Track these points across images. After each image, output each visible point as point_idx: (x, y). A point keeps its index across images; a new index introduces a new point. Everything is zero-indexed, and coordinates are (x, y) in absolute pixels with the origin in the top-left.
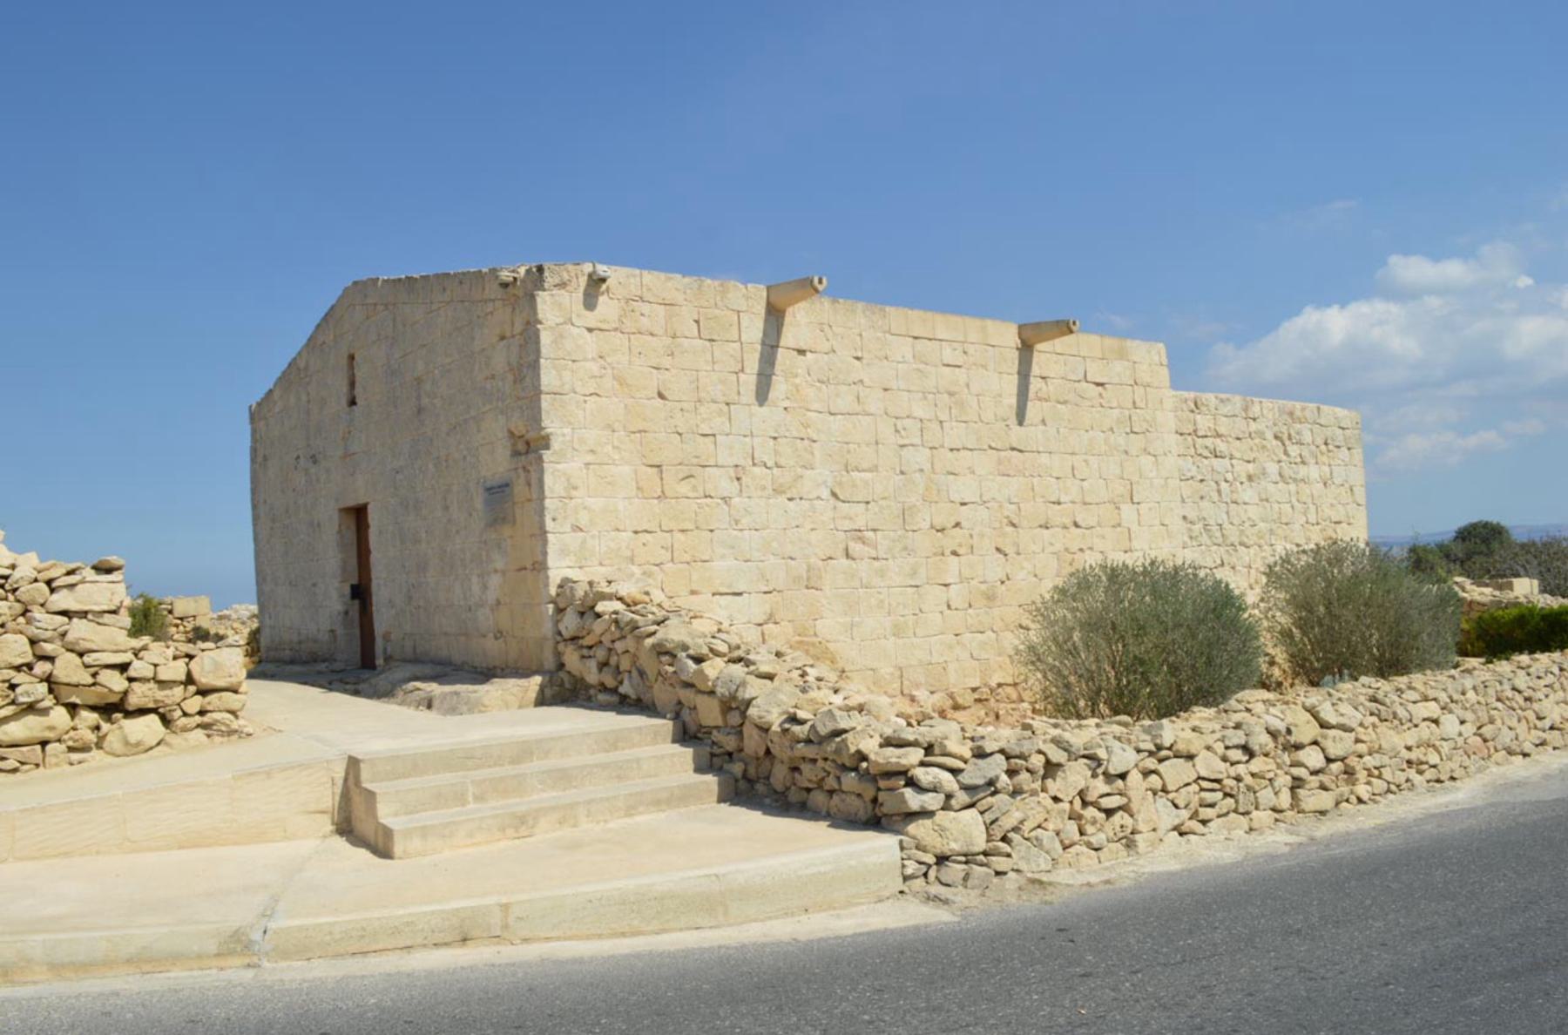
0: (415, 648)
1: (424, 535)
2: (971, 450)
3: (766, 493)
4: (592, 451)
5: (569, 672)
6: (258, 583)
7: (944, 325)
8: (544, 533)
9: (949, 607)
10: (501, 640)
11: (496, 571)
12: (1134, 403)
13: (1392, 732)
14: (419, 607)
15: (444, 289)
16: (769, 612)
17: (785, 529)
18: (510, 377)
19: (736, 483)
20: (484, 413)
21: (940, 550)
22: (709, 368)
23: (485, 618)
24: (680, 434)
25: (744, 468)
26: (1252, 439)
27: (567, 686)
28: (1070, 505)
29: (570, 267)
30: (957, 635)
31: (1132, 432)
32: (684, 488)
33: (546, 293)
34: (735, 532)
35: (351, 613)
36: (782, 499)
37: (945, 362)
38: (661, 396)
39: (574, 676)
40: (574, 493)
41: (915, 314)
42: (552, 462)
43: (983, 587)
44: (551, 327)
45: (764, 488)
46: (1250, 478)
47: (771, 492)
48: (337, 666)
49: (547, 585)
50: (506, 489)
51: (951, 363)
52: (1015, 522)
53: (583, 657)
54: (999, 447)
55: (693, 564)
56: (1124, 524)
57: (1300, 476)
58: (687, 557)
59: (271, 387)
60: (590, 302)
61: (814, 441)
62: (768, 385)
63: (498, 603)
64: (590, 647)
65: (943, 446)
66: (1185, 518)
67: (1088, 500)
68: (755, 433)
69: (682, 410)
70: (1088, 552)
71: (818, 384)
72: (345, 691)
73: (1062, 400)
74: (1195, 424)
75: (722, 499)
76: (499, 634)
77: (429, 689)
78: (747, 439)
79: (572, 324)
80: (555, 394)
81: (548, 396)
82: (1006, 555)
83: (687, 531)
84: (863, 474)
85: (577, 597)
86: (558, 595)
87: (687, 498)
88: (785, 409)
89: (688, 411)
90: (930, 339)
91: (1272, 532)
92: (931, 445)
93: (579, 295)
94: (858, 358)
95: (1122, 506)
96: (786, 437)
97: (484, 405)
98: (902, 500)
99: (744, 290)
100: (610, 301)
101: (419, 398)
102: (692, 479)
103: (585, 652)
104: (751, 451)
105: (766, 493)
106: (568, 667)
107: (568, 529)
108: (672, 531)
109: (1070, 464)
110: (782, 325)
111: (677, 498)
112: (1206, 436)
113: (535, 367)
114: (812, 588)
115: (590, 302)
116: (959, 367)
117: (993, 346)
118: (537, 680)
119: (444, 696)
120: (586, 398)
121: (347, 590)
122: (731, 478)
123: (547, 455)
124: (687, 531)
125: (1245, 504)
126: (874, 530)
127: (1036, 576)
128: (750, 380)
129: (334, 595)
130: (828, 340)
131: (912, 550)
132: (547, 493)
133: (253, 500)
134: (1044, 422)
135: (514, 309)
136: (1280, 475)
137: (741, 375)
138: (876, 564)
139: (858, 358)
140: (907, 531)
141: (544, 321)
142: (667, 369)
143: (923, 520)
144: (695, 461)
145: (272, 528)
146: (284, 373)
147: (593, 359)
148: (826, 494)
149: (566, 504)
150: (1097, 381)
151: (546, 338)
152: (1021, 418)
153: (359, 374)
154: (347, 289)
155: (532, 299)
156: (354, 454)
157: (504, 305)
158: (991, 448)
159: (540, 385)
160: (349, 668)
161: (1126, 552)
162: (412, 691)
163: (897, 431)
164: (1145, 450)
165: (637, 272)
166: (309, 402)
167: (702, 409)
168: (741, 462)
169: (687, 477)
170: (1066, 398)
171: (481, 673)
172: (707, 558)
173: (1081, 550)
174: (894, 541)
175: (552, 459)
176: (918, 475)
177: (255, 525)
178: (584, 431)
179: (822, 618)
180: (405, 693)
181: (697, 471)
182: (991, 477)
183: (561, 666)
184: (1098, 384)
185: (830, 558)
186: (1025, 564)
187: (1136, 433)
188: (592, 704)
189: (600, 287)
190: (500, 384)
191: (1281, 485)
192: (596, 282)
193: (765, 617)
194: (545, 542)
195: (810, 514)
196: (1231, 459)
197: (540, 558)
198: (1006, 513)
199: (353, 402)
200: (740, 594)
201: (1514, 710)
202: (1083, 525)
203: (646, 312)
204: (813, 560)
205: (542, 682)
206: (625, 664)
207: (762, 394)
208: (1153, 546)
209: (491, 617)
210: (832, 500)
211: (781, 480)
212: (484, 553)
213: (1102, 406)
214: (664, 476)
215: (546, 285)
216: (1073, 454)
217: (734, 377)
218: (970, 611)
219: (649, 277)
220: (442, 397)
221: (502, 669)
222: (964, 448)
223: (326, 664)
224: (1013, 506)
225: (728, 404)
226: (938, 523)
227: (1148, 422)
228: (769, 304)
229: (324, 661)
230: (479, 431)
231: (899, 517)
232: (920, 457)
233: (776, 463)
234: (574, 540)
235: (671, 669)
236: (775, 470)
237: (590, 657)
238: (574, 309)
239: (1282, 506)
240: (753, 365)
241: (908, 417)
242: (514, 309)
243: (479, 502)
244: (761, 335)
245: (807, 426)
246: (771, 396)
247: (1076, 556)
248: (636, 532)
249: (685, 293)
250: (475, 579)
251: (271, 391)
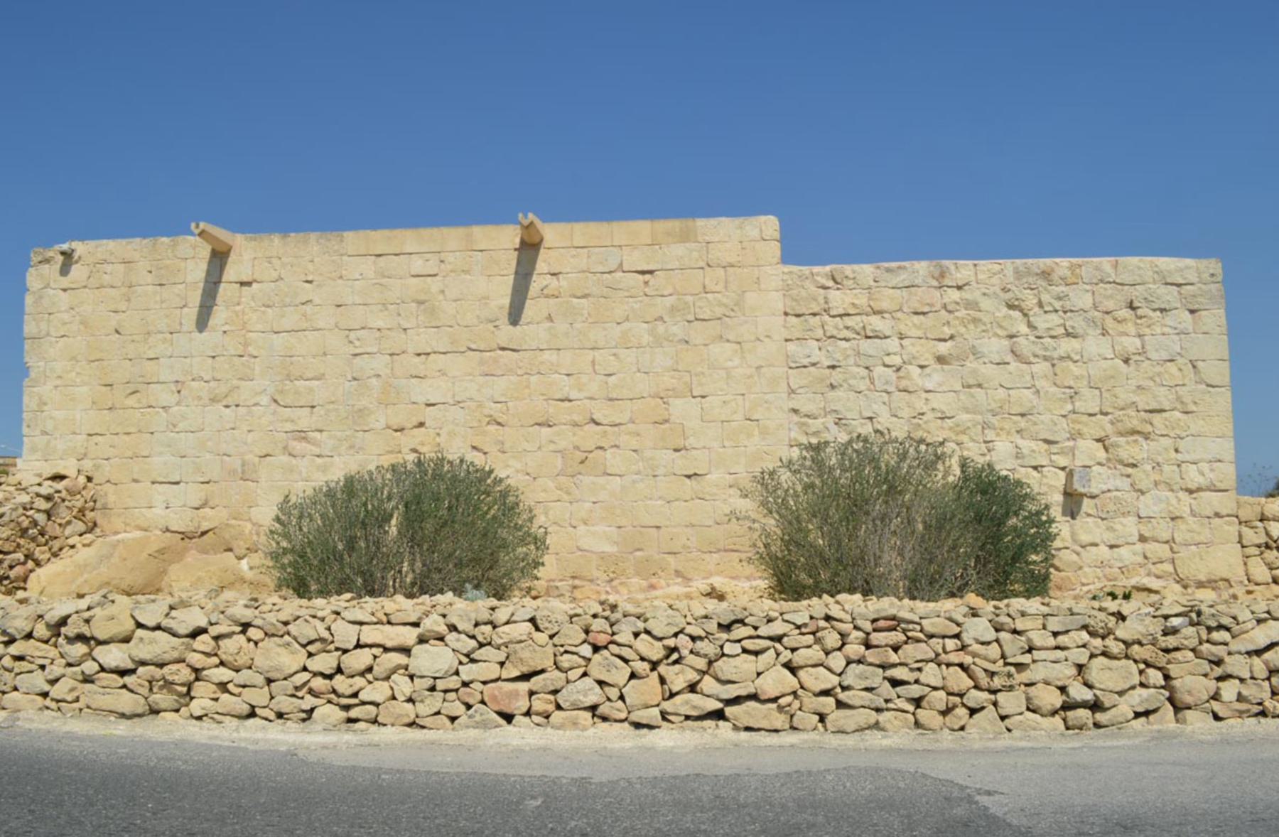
3: (201, 402)
4: (60, 377)
7: (409, 239)
12: (704, 287)
13: (282, 650)
16: (204, 498)
19: (176, 394)
22: (158, 307)
26: (950, 312)
31: (697, 319)
32: (131, 401)
36: (220, 406)
37: (413, 273)
38: (117, 332)
40: (45, 408)
44: (34, 292)
45: (200, 398)
46: (941, 360)
47: (207, 402)
52: (500, 420)
57: (1062, 352)
58: (129, 454)
60: (65, 271)
61: (255, 357)
62: (208, 314)
66: (795, 411)
71: (263, 309)
73: (579, 294)
74: (826, 303)
78: (188, 360)
84: (307, 382)
88: (225, 332)
91: (986, 426)
95: (671, 400)
105: (201, 402)
107: (38, 432)
108: (117, 434)
109: (591, 359)
110: (225, 263)
112: (848, 315)
117: (481, 251)
122: (173, 392)
123: (26, 382)
127: (528, 474)
128: (192, 313)
131: (361, 448)
132: (25, 408)
134: (550, 318)
138: (319, 460)
139: (307, 282)
143: (378, 420)
144: (141, 379)
147: (66, 311)
148: (265, 400)
150: (639, 269)
152: (515, 316)
161: (676, 450)
164: (721, 337)
170: (587, 292)
173: (601, 448)
174: (339, 440)
176: (374, 381)
179: (257, 506)
184: (643, 273)
191: (1014, 365)
193: (200, 503)
198: (486, 412)
200: (177, 483)
201: (626, 661)
202: (605, 422)
203: (108, 271)
204: (247, 457)
208: (726, 444)
210: (274, 405)
211: (217, 391)
219: (110, 245)
222: (435, 353)
224: (499, 405)
226: (395, 423)
227: (726, 306)
232: (380, 363)
234: (41, 441)
236: (212, 384)
239: (1011, 392)
241: (363, 328)
244: (203, 275)
245: (246, 345)
246: (211, 323)
247: (590, 456)
248: (90, 435)
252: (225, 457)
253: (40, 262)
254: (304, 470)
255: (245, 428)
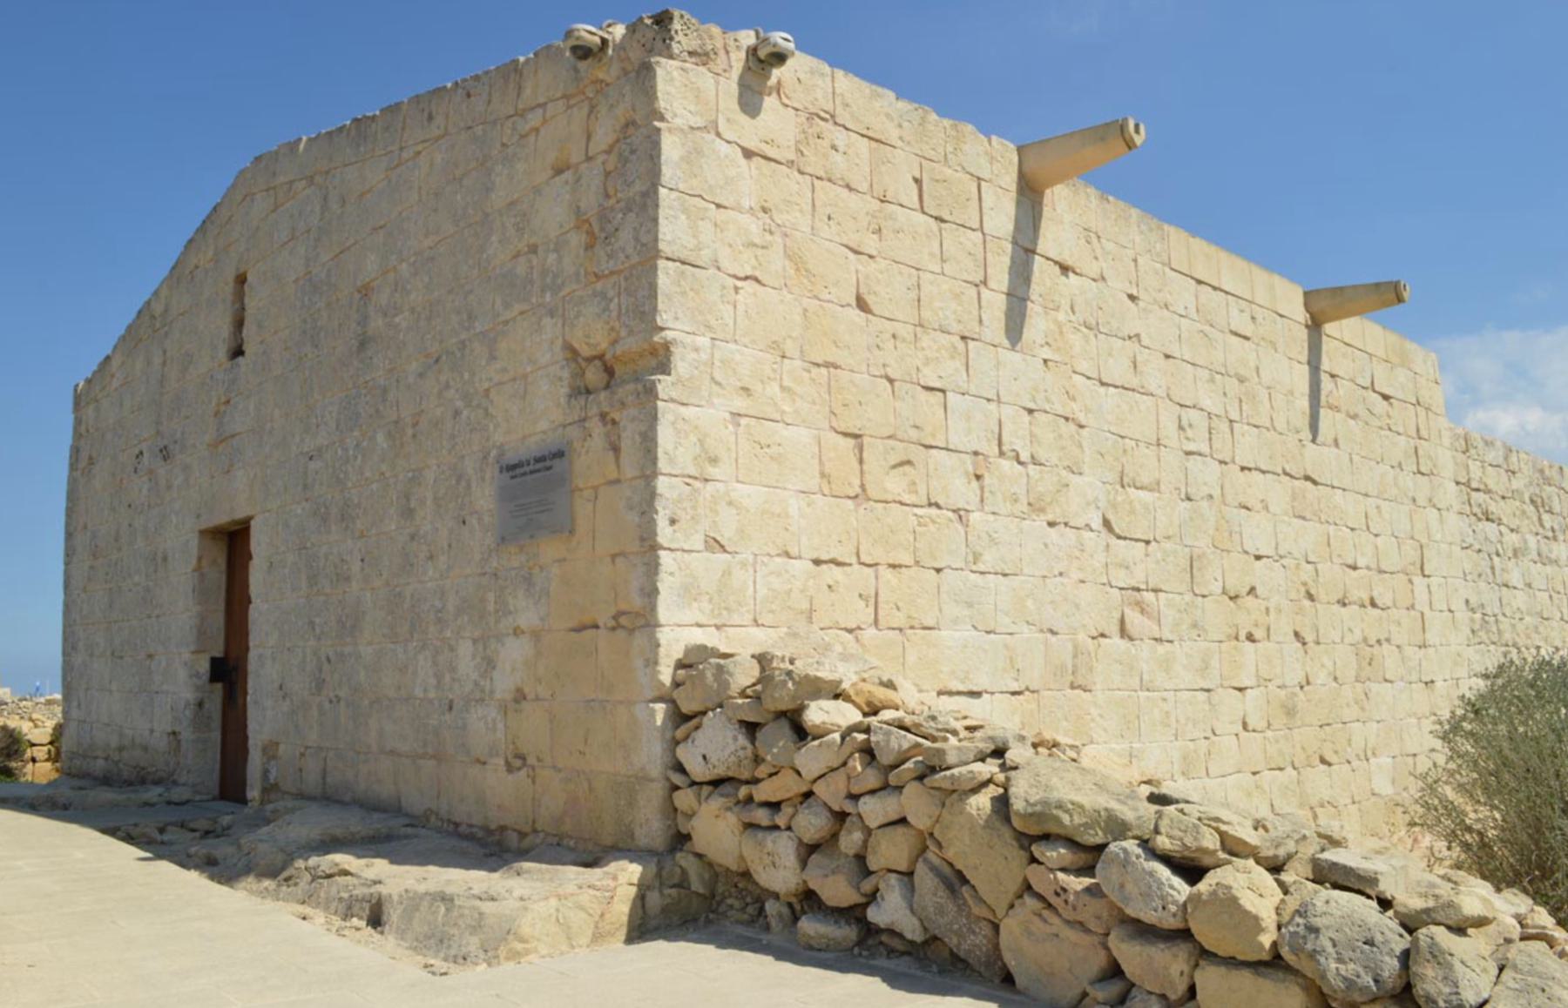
0: (324, 773)
1: (356, 567)
2: (1264, 472)
4: (746, 390)
5: (699, 856)
6: (65, 654)
8: (655, 548)
9: (1245, 726)
10: (523, 773)
11: (517, 632)
14: (339, 699)
15: (430, 118)
17: (1045, 577)
18: (577, 240)
19: (975, 484)
20: (506, 323)
21: (1232, 632)
23: (484, 726)
24: (891, 381)
25: (986, 457)
27: (696, 886)
28: (1365, 571)
29: (716, 30)
30: (1254, 773)
32: (895, 485)
33: (671, 62)
34: (973, 576)
35: (207, 706)
36: (1040, 523)
38: (862, 305)
39: (710, 865)
41: (1198, 244)
42: (672, 400)
43: (1283, 693)
47: (1025, 508)
48: (178, 794)
49: (652, 662)
50: (556, 462)
51: (1240, 332)
53: (750, 826)
54: (1293, 473)
55: (909, 632)
56: (1417, 607)
58: (899, 619)
59: (109, 351)
60: (750, 100)
61: (1082, 427)
63: (520, 696)
64: (775, 806)
65: (1234, 462)
66: (1467, 601)
67: (1383, 567)
68: (1003, 399)
69: (894, 336)
70: (1385, 645)
72: (185, 861)
75: (954, 511)
76: (517, 761)
77: (370, 874)
79: (718, 135)
80: (683, 263)
81: (670, 264)
82: (1304, 644)
83: (900, 566)
85: (734, 689)
86: (677, 684)
87: (902, 504)
88: (1045, 361)
89: (904, 340)
90: (1215, 288)
92: (1220, 457)
93: (731, 86)
94: (1132, 298)
96: (1046, 412)
97: (507, 306)
98: (1189, 543)
99: (986, 144)
100: (781, 108)
101: (364, 321)
102: (907, 468)
103: (762, 816)
104: (996, 430)
106: (700, 842)
107: (697, 542)
108: (876, 564)
111: (887, 502)
113: (644, 207)
114: (1080, 687)
115: (750, 100)
116: (1246, 338)
118: (627, 874)
119: (413, 902)
120: (739, 284)
121: (204, 666)
122: (967, 473)
123: (665, 385)
124: (900, 566)
125: (1515, 588)
126: (1156, 591)
128: (995, 303)
129: (182, 674)
130: (1096, 258)
132: (662, 465)
133: (68, 525)
135: (592, 109)
136: (1539, 555)
137: (983, 289)
138: (1161, 649)
139: (1132, 298)
140: (1196, 595)
141: (668, 116)
142: (871, 257)
144: (914, 434)
145: (92, 567)
146: (129, 328)
149: (697, 491)
151: (671, 149)
153: (251, 304)
154: (242, 172)
155: (645, 72)
156: (233, 436)
157: (569, 107)
158: (1286, 474)
159: (656, 240)
160: (198, 798)
162: (329, 876)
163: (1181, 428)
165: (827, 69)
166: (164, 364)
167: (925, 341)
168: (983, 447)
169: (902, 464)
171: (470, 837)
172: (930, 623)
173: (1379, 641)
175: (674, 395)
177: (67, 564)
178: (732, 346)
180: (314, 878)
181: (917, 454)
182: (1286, 518)
183: (681, 839)
185: (1103, 635)
186: (1325, 660)
187: (1423, 474)
188: (765, 938)
189: (768, 77)
190: (552, 257)
192: (765, 61)
194: (653, 568)
195: (1078, 554)
196: (1499, 524)
197: (637, 602)
199: (238, 352)
203: (840, 144)
204: (1082, 637)
205: (643, 876)
206: (891, 851)
207: (1015, 326)
209: (500, 726)
210: (1104, 531)
212: (491, 596)
213: (1390, 429)
214: (865, 455)
215: (676, 48)
216: (1366, 495)
217: (973, 291)
218: (1269, 734)
219: (845, 82)
220: (413, 310)
221: (522, 835)
222: (1256, 469)
223: (159, 790)
225: (963, 338)
228: (1022, 176)
229: (157, 782)
230: (493, 357)
231: (1185, 570)
233: (1033, 457)
234: (707, 566)
235: (1077, 883)
236: (1031, 467)
237: (776, 828)
238: (722, 106)
240: (1000, 278)
242: (592, 109)
243: (485, 497)
244: (1011, 227)
246: (1025, 336)
248: (817, 562)
249: (900, 126)
250: (465, 649)
251: (108, 358)
252: (1049, 635)
253: (691, 53)
254: (1145, 667)
255: (1076, 575)
